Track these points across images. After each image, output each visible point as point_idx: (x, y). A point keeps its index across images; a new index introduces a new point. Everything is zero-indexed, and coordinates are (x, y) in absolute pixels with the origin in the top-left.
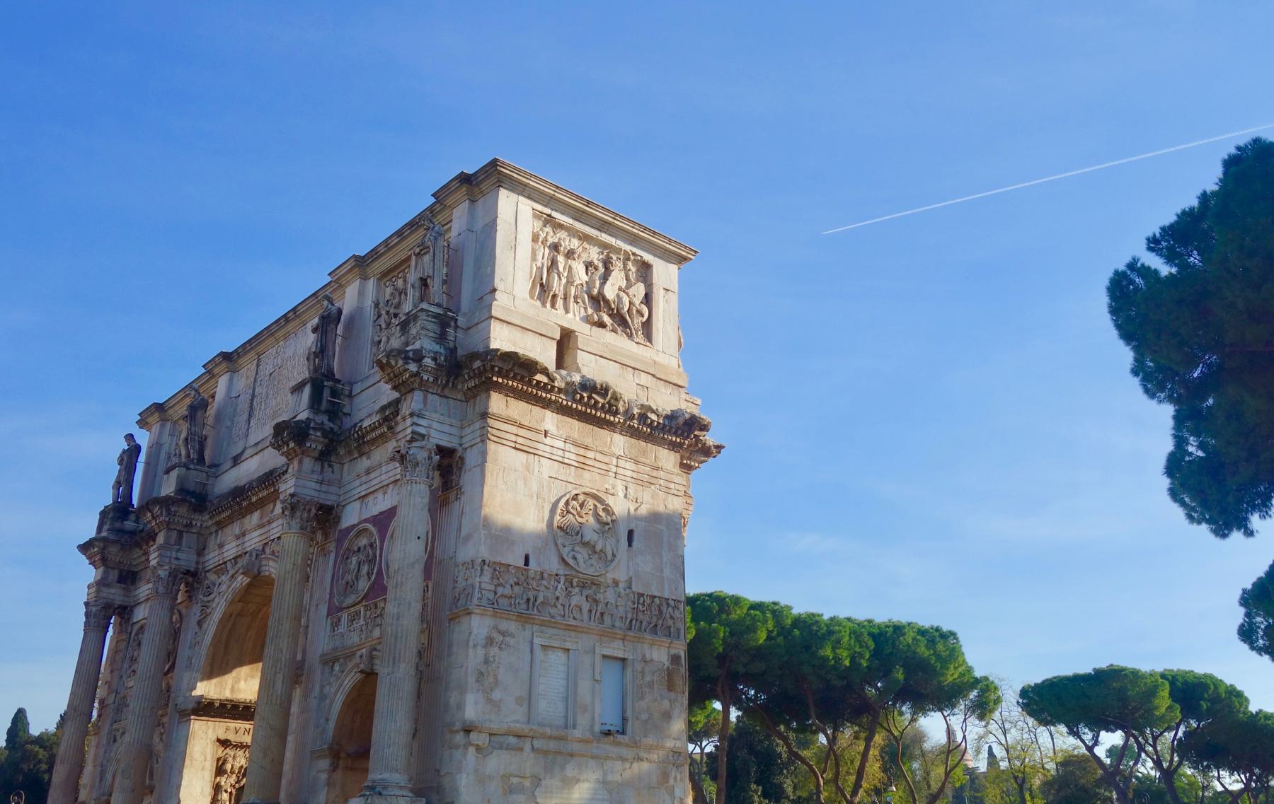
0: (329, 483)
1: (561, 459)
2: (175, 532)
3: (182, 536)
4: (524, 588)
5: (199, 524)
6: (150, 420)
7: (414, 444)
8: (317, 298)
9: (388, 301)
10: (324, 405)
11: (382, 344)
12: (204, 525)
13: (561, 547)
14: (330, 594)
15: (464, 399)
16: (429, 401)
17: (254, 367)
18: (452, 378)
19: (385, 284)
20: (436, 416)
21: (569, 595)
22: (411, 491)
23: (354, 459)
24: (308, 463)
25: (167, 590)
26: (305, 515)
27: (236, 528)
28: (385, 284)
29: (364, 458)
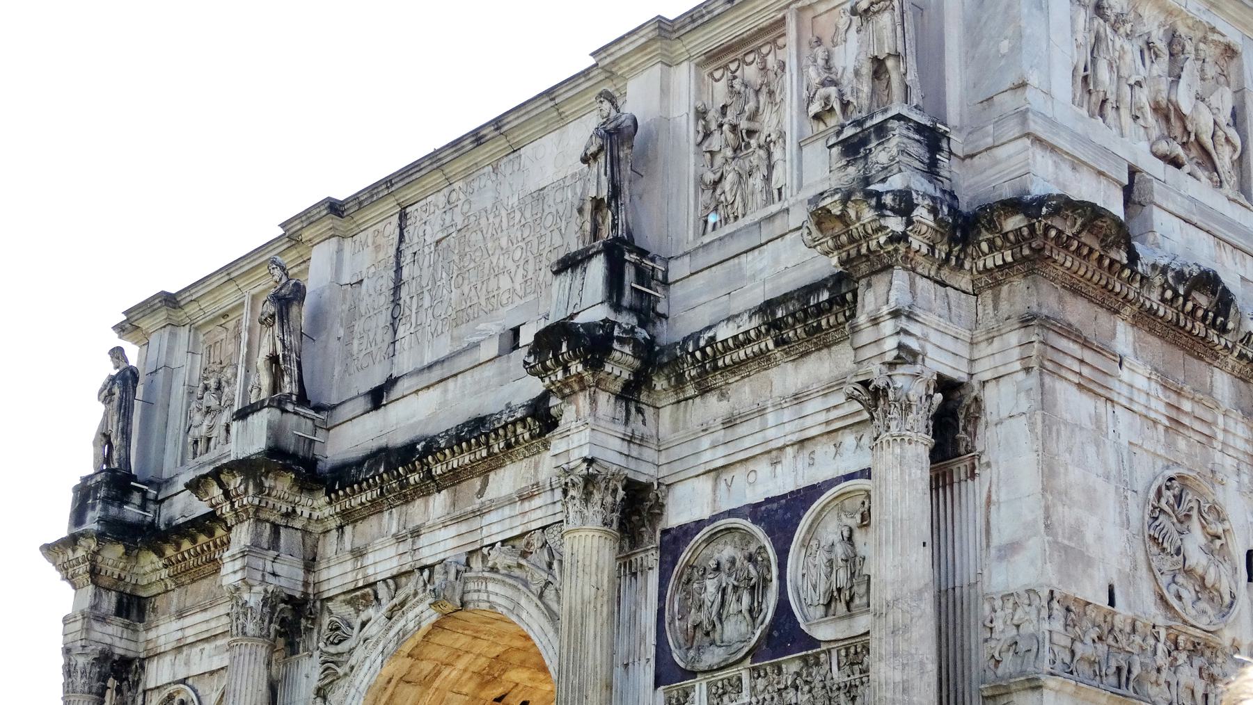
0: (642, 441)
1: (1144, 411)
2: (268, 525)
3: (279, 533)
4: (1109, 646)
5: (306, 515)
6: (145, 324)
7: (901, 369)
8: (553, 99)
9: (724, 107)
10: (628, 298)
11: (727, 185)
12: (315, 515)
13: (1158, 574)
14: (657, 646)
15: (970, 289)
16: (918, 291)
17: (392, 227)
18: (957, 249)
19: (711, 75)
20: (932, 319)
21: (1174, 667)
22: (902, 457)
23: (686, 399)
24: (605, 402)
25: (261, 629)
26: (609, 499)
27: (391, 521)
28: (711, 75)
29: (712, 399)
